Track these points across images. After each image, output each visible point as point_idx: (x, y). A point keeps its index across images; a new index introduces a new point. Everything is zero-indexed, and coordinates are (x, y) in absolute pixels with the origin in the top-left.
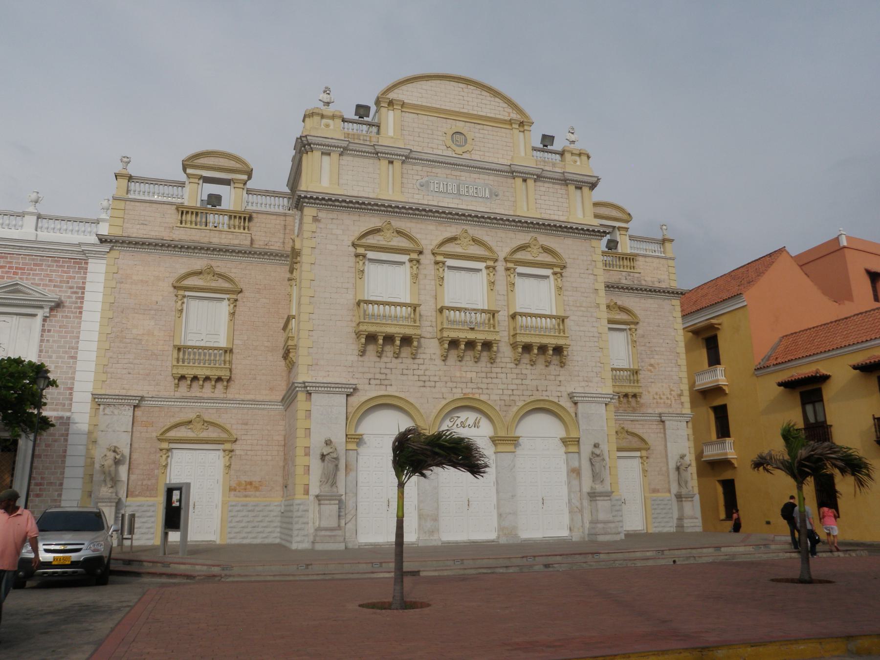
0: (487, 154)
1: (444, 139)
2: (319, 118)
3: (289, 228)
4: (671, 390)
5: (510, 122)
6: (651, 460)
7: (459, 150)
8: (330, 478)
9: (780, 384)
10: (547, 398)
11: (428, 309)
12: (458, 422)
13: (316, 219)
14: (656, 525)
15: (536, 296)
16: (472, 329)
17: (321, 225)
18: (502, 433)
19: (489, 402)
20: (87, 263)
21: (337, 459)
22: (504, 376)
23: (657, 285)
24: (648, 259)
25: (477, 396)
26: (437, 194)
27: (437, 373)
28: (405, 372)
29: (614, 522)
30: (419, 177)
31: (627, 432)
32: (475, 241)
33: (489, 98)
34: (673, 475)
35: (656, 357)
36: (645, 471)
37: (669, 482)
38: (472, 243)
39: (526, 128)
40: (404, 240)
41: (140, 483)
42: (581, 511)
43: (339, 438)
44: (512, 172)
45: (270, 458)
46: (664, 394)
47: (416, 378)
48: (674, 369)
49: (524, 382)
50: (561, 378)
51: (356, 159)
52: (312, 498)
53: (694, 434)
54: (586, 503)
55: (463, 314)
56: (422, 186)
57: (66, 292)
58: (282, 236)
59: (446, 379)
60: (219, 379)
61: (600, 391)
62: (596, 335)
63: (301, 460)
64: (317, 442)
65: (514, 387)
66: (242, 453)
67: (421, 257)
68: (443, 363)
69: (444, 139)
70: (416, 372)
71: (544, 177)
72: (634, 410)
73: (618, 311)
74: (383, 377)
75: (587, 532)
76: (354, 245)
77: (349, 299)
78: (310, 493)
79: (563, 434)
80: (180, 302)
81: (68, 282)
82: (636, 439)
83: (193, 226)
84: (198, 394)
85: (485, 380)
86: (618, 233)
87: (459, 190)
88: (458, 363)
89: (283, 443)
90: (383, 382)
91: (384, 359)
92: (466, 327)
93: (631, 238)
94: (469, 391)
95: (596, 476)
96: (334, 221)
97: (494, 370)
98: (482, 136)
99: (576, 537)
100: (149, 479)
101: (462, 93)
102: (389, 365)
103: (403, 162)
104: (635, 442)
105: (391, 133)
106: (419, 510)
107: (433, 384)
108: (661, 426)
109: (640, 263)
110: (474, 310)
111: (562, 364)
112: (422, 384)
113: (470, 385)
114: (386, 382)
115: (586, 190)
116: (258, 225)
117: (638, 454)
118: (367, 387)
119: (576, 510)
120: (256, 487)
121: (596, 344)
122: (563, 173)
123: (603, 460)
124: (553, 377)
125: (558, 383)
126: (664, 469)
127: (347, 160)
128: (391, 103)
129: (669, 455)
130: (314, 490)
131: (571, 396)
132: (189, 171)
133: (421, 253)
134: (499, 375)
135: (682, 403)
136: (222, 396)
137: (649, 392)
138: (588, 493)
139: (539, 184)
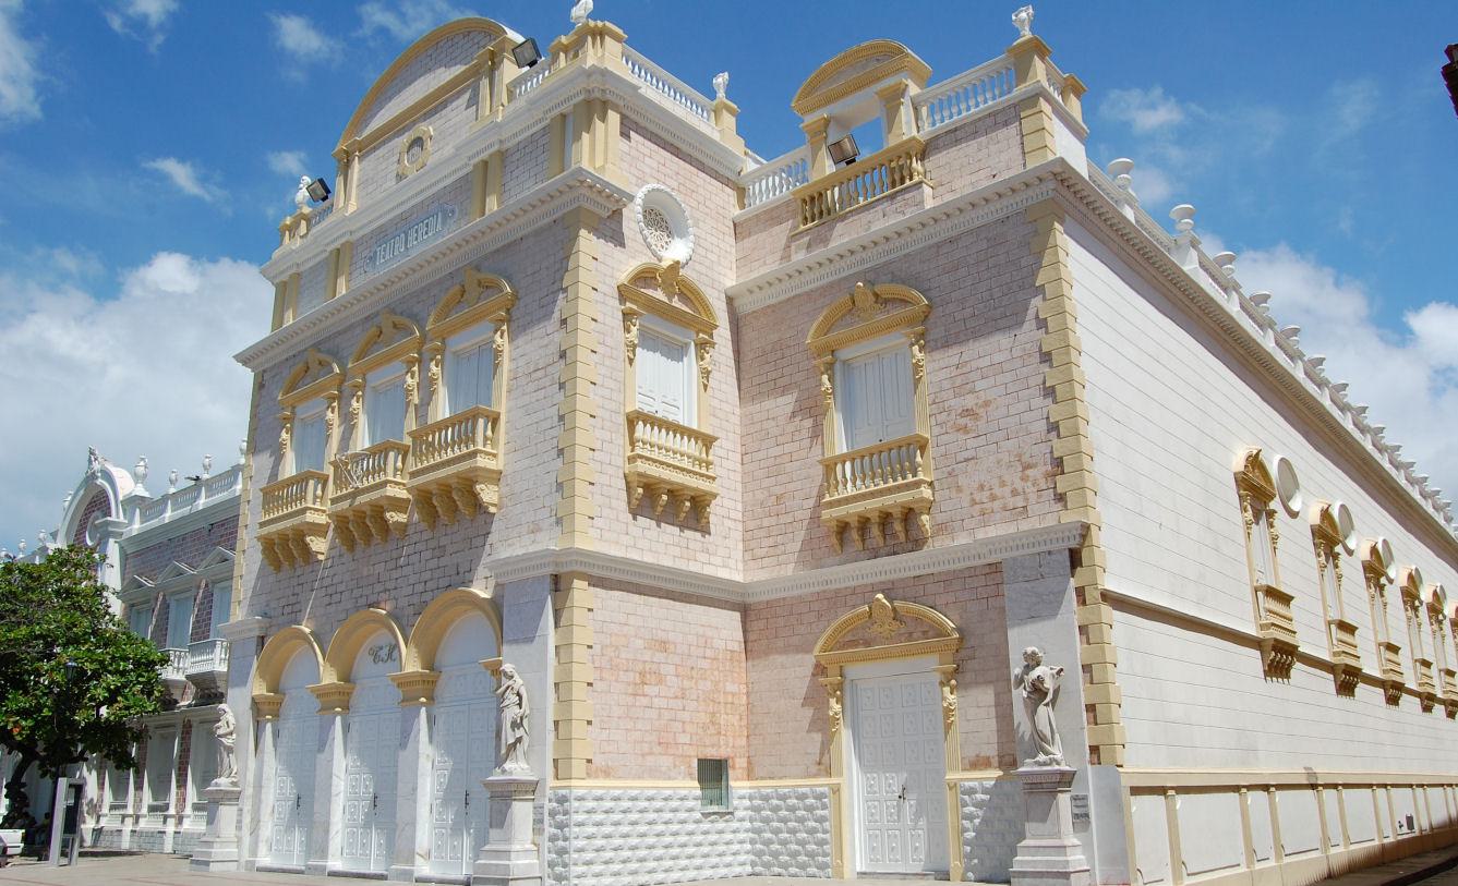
17: (264, 392)
35: (980, 385)
46: (1003, 484)
65: (427, 575)
113: (379, 587)
137: (959, 489)
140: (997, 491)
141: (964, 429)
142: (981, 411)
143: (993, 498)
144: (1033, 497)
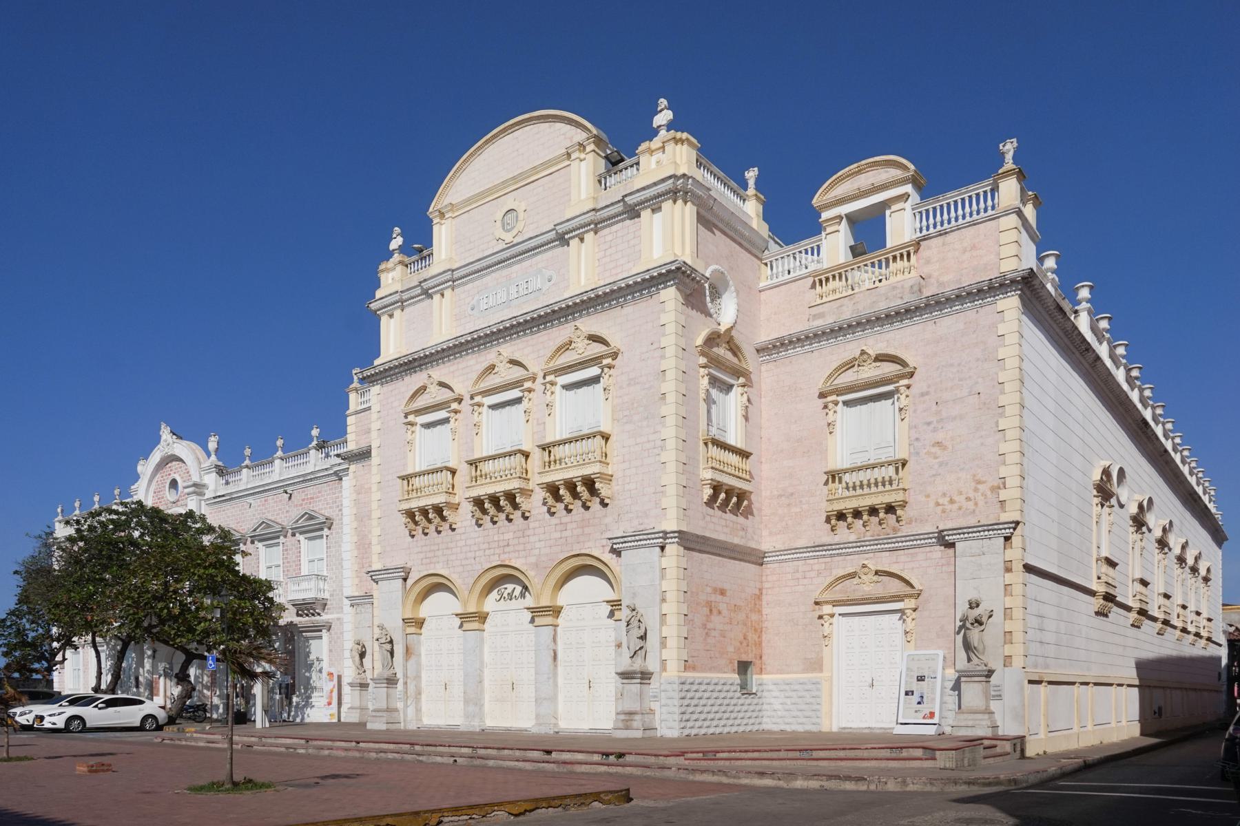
46: (961, 493)
62: (659, 443)
85: (522, 540)
140: (956, 498)
144: (981, 503)
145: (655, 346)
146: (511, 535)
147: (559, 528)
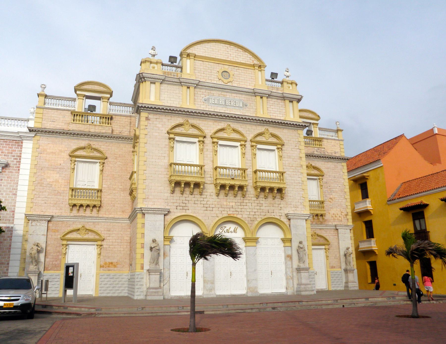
0: (241, 83)
1: (217, 75)
2: (149, 63)
3: (132, 123)
4: (342, 212)
5: (254, 66)
6: (330, 250)
7: (226, 81)
8: (155, 261)
9: (401, 209)
10: (274, 217)
11: (209, 168)
12: (225, 230)
13: (147, 119)
14: (333, 286)
15: (268, 160)
16: (233, 179)
17: (150, 122)
18: (249, 236)
19: (242, 219)
20: (22, 143)
21: (159, 250)
22: (250, 204)
23: (334, 155)
24: (329, 141)
25: (235, 216)
26: (214, 105)
27: (214, 203)
28: (196, 202)
29: (310, 284)
30: (204, 96)
31: (317, 235)
32: (234, 130)
33: (242, 53)
34: (343, 259)
35: (333, 194)
36: (327, 257)
37: (340, 262)
38: (232, 131)
39: (262, 69)
40: (196, 130)
41: (51, 263)
42: (292, 278)
43: (160, 239)
44: (255, 93)
45: (122, 249)
46: (338, 215)
47: (202, 205)
48: (343, 201)
49: (261, 208)
50: (281, 206)
51: (169, 86)
52: (145, 271)
53: (354, 236)
54: (295, 274)
55: (228, 170)
56: (205, 100)
57: (11, 158)
58: (129, 128)
59: (218, 206)
60: (94, 206)
61: (302, 213)
62: (301, 182)
63: (139, 251)
64: (148, 241)
65: (256, 210)
66: (107, 246)
67: (205, 139)
68: (217, 197)
69: (217, 75)
70: (202, 202)
71: (272, 96)
72: (321, 223)
73: (313, 169)
74: (184, 205)
75: (295, 290)
76: (168, 133)
77: (166, 162)
78: (144, 268)
79: (283, 236)
80: (73, 164)
81: (12, 153)
82: (322, 239)
83: (80, 122)
84: (83, 215)
85: (240, 207)
86: (312, 126)
87: (225, 103)
88: (225, 197)
89: (129, 241)
90: (184, 208)
91: (185, 195)
92: (229, 178)
93: (320, 129)
94: (231, 212)
95: (300, 259)
96: (158, 120)
97: (245, 201)
98: (238, 73)
99: (290, 292)
100: (56, 261)
101: (227, 50)
102: (187, 199)
103: (195, 87)
104: (322, 241)
105: (188, 71)
106: (204, 278)
107: (211, 209)
108: (336, 232)
109: (325, 142)
110: (234, 168)
111: (282, 198)
112: (205, 209)
113: (232, 209)
114: (186, 208)
115: (295, 103)
116: (116, 122)
117: (323, 247)
118: (175, 210)
119: (289, 278)
120: (114, 265)
121: (301, 187)
122: (283, 93)
123: (305, 250)
124: (277, 205)
125: (280, 208)
126: (338, 255)
127: (164, 86)
128: (188, 55)
129: (341, 248)
130: (146, 267)
131: (287, 215)
132: (78, 92)
133: (205, 137)
134: (248, 204)
135: (348, 219)
136: (96, 215)
137: (329, 213)
138: (296, 269)
139: (269, 99)
141: (330, 202)
142: (334, 199)
143: (336, 217)
145: (297, 147)
146: (234, 204)
147: (259, 205)
